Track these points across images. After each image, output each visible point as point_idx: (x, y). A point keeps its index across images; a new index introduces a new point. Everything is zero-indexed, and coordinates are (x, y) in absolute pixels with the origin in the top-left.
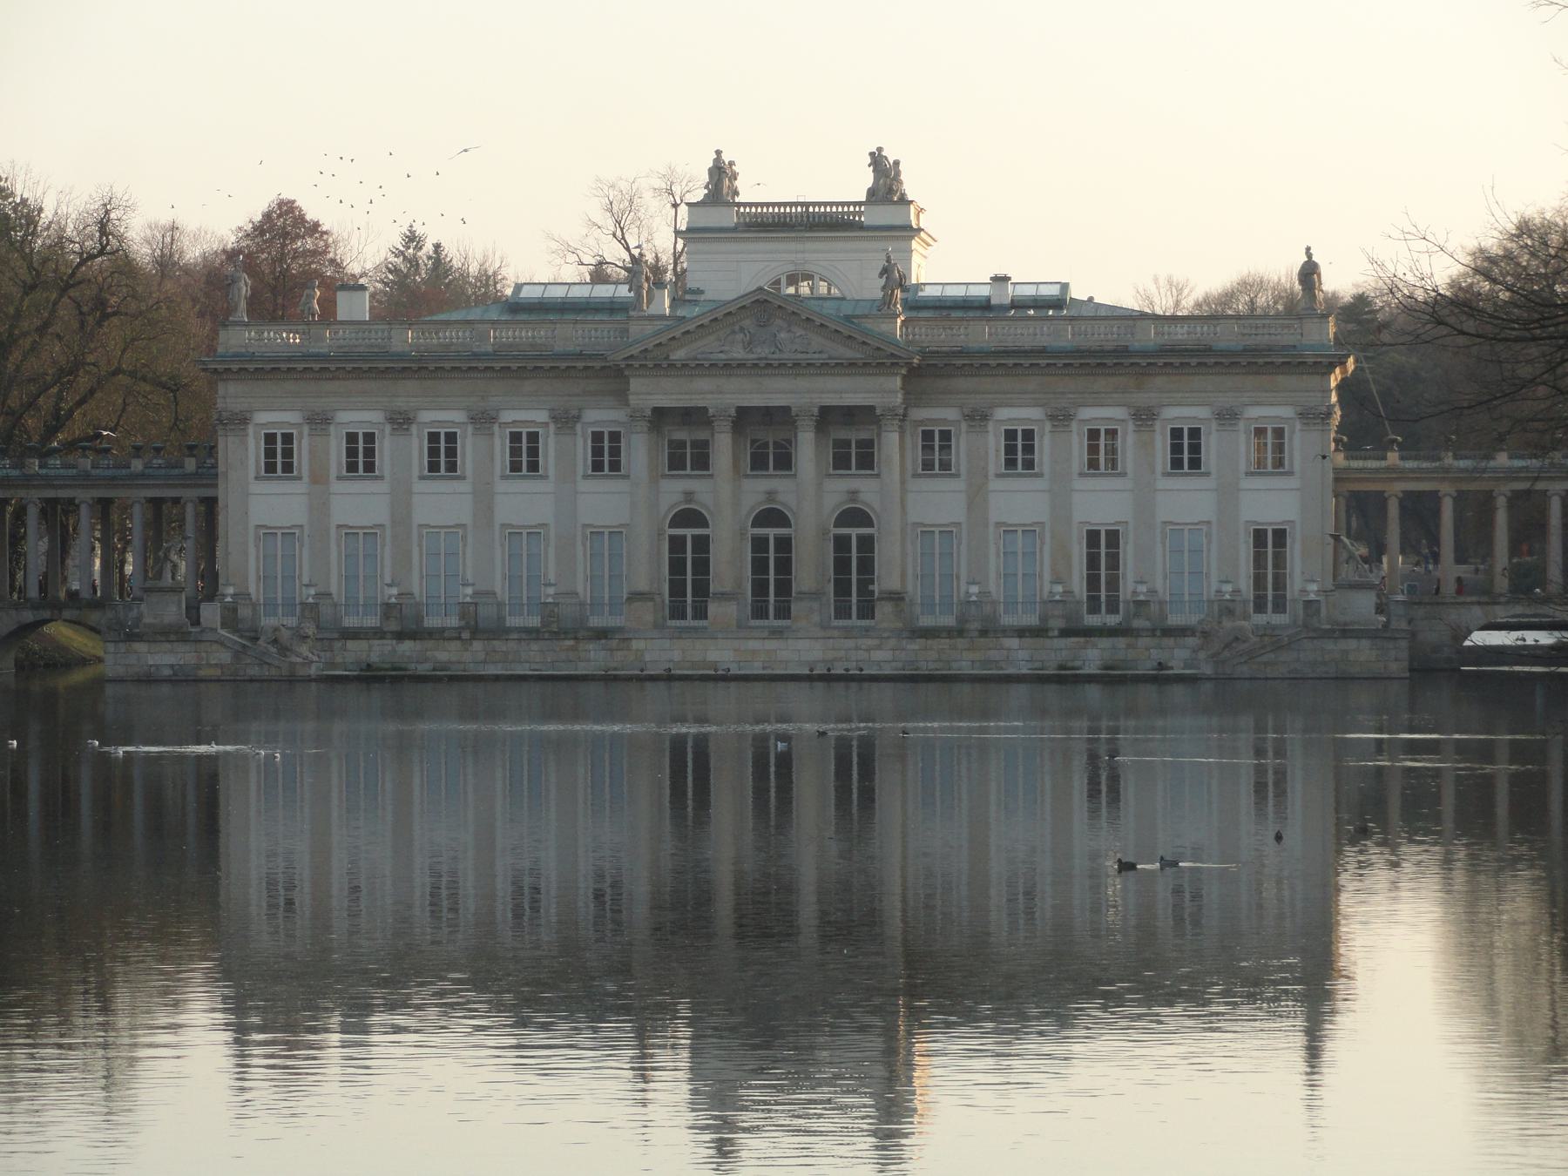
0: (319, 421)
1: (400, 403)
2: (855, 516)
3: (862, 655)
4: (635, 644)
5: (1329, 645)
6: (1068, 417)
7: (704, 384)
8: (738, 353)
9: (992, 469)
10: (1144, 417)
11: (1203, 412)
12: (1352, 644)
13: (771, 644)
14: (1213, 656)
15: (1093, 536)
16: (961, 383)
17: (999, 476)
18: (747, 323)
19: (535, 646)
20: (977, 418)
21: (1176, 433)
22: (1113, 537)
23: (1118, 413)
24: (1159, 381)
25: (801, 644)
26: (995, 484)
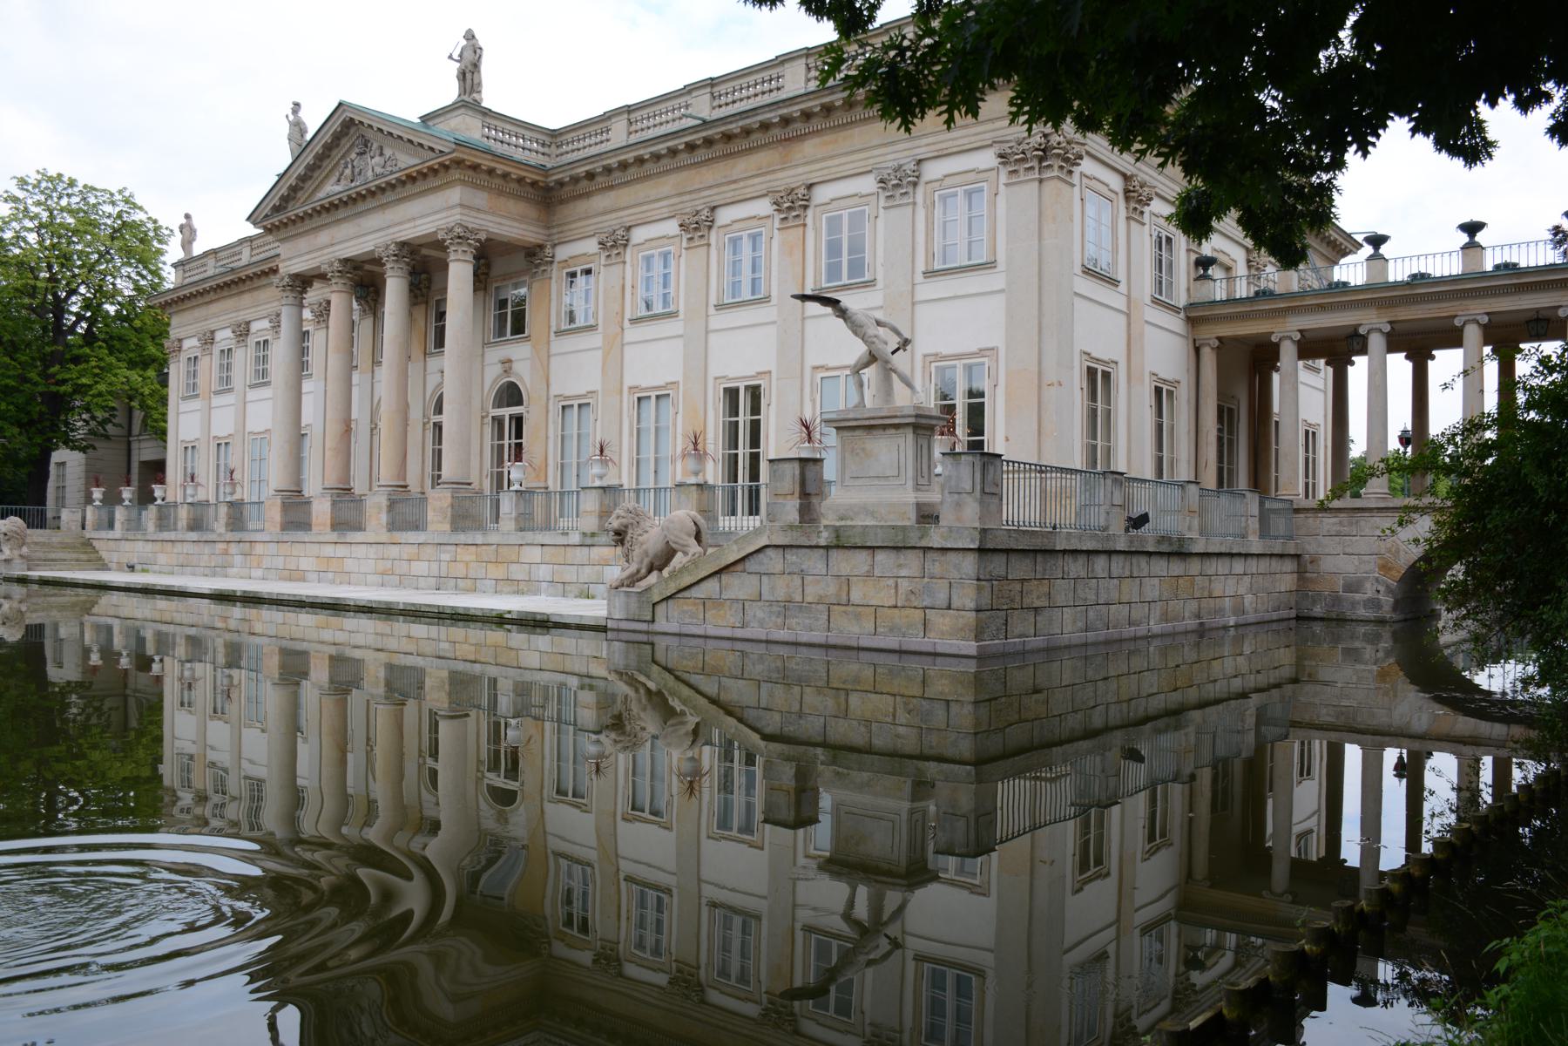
0: (208, 340)
1: (243, 316)
2: (511, 394)
3: (402, 567)
4: (259, 549)
5: (814, 562)
6: (711, 224)
7: (323, 237)
8: (332, 189)
9: (628, 315)
10: (793, 205)
12: (860, 560)
13: (341, 551)
14: (634, 579)
15: (732, 394)
16: (599, 202)
17: (634, 321)
18: (353, 156)
19: (207, 549)
20: (616, 244)
21: (834, 225)
22: (755, 393)
24: (810, 147)
25: (361, 551)
26: (632, 333)
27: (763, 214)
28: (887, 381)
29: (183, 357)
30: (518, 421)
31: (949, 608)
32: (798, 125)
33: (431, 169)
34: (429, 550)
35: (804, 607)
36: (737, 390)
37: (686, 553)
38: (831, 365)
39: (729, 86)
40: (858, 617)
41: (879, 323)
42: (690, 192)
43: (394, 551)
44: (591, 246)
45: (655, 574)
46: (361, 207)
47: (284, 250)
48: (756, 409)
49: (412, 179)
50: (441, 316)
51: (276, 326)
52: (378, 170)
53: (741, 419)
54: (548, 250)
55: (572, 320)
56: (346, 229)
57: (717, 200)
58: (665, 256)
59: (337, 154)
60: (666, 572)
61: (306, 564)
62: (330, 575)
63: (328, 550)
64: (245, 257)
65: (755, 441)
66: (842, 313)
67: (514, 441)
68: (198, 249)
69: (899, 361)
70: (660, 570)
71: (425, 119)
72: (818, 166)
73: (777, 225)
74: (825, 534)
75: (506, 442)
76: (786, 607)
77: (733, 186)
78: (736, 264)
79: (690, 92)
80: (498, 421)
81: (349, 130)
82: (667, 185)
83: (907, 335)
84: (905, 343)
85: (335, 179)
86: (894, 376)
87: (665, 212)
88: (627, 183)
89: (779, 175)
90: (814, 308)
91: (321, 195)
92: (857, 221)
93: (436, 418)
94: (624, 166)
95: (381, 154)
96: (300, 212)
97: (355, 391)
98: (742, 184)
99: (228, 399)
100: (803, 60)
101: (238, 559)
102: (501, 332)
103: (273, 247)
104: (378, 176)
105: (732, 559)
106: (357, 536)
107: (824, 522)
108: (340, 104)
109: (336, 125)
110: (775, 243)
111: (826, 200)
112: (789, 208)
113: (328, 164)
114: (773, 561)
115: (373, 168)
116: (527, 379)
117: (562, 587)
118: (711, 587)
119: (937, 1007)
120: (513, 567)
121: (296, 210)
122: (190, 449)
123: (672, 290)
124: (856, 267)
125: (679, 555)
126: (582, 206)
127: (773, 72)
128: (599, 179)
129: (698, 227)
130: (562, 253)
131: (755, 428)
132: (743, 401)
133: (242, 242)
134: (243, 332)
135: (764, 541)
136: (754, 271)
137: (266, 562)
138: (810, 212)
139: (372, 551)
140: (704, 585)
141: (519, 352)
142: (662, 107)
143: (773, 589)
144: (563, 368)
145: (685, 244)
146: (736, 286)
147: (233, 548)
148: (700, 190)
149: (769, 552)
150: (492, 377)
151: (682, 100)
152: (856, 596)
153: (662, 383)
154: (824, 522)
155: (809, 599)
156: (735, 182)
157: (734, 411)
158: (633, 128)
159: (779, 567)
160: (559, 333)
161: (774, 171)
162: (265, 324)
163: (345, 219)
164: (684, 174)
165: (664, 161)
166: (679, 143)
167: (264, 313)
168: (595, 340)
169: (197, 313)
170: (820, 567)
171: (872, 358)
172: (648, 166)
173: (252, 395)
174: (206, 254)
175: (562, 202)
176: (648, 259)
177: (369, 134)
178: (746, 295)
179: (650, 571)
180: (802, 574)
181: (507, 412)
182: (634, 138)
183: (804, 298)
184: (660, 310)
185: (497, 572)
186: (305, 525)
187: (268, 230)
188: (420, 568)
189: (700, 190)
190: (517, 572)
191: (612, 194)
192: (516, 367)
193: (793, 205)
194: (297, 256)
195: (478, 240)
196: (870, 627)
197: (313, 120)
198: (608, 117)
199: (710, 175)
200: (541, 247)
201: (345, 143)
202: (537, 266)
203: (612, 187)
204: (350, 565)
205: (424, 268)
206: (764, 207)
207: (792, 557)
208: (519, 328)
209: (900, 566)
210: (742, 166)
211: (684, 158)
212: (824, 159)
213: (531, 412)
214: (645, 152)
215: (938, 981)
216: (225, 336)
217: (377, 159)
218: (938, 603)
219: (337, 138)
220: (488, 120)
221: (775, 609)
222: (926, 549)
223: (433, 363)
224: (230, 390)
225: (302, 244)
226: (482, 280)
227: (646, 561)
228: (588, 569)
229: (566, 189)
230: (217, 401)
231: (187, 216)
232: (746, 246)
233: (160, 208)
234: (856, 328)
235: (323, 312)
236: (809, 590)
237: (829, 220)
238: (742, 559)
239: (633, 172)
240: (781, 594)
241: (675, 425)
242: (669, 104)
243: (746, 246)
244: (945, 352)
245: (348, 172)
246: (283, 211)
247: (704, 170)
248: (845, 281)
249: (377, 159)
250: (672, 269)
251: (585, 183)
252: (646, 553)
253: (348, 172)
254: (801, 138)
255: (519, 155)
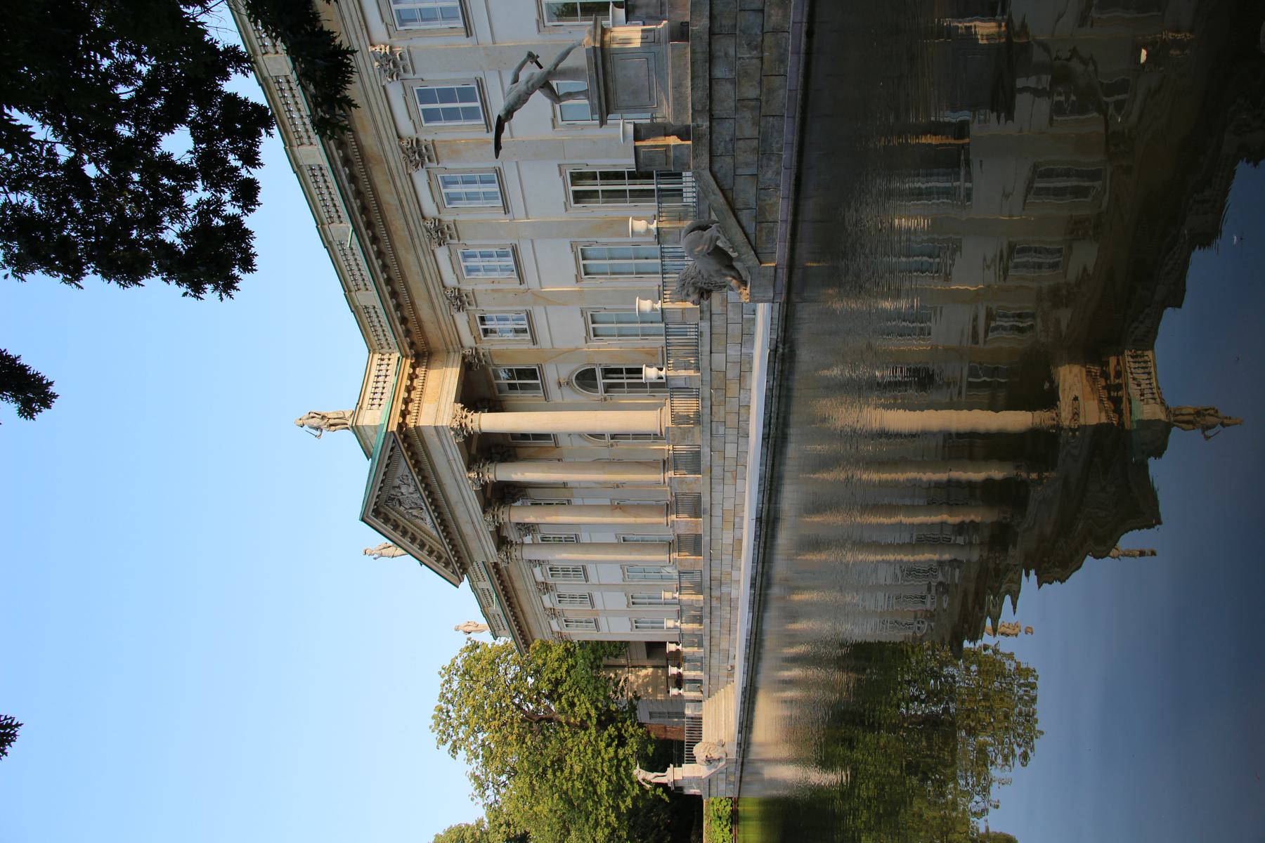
0: (553, 613)
1: (532, 587)
2: (586, 379)
3: (730, 464)
4: (716, 574)
5: (725, 131)
7: (467, 529)
8: (427, 523)
11: (395, 91)
13: (717, 511)
15: (579, 197)
16: (425, 312)
17: (521, 281)
19: (716, 613)
20: (459, 300)
21: (430, 116)
22: (577, 177)
23: (420, 178)
24: (368, 140)
25: (717, 497)
27: (426, 177)
28: (566, 74)
29: (565, 631)
30: (608, 372)
31: (762, 11)
32: (350, 152)
33: (407, 450)
34: (715, 443)
35: (763, 138)
36: (575, 192)
37: (718, 238)
38: (551, 115)
39: (322, 210)
40: (771, 91)
41: (516, 80)
42: (412, 239)
43: (717, 471)
44: (461, 319)
45: (736, 264)
46: (442, 502)
47: (479, 558)
48: (593, 176)
49: (417, 464)
50: (525, 436)
51: (539, 563)
52: (412, 489)
53: (600, 188)
54: (467, 352)
55: (525, 331)
56: (460, 512)
57: (417, 215)
58: (466, 256)
59: (402, 522)
60: (734, 255)
61: (727, 537)
62: (737, 520)
63: (717, 521)
64: (486, 585)
65: (618, 176)
66: (509, 113)
67: (624, 375)
68: (482, 621)
69: (547, 63)
70: (731, 259)
71: (368, 455)
72: (382, 132)
73: (434, 165)
74: (699, 121)
75: (625, 381)
76: (764, 153)
77: (405, 203)
78: (471, 197)
79: (330, 243)
80: (608, 387)
81: (381, 510)
82: (408, 258)
83: (525, 56)
84: (532, 57)
85: (419, 521)
86: (561, 66)
87: (430, 258)
88: (408, 291)
89: (393, 164)
90: (505, 136)
91: (435, 533)
92: (425, 96)
93: (608, 438)
94: (394, 294)
95: (399, 487)
96: (448, 548)
97: (588, 502)
98: (402, 196)
99: (597, 597)
100: (295, 149)
101: (725, 589)
102: (536, 387)
103: (477, 567)
104: (417, 489)
105: (721, 200)
106: (705, 499)
107: (689, 122)
108: (363, 520)
109: (379, 523)
110: (450, 166)
111: (411, 124)
112: (420, 155)
113: (411, 529)
114: (724, 164)
115: (409, 491)
116: (574, 367)
117: (747, 336)
118: (745, 216)
119: (1059, 192)
120: (729, 375)
121: (446, 550)
122: (637, 625)
123: (494, 250)
124: (466, 95)
125: (719, 244)
126: (430, 327)
127: (308, 174)
128: (406, 314)
129: (441, 233)
130: (468, 340)
131: (606, 176)
132: (586, 186)
133: (474, 589)
134: (546, 588)
135: (707, 174)
136: (475, 182)
137: (727, 568)
138: (422, 138)
139: (717, 488)
140: (745, 222)
141: (552, 374)
142: (344, 264)
143: (747, 165)
144: (563, 337)
145: (456, 241)
146: (488, 196)
147: (716, 593)
148: (410, 231)
149: (716, 167)
150: (571, 396)
151: (337, 249)
152: (752, 93)
153: (572, 256)
154: (689, 122)
155: (756, 134)
156: (401, 202)
157: (591, 195)
158: (362, 286)
159: (728, 160)
160: (534, 340)
161: (390, 169)
162: (537, 571)
163: (452, 513)
164: (397, 244)
165: (388, 262)
166: (372, 250)
167: (529, 572)
168: (539, 314)
169: (531, 621)
170: (728, 124)
171: (545, 85)
172: (393, 275)
173: (593, 579)
174: (486, 615)
175: (427, 343)
176: (470, 270)
177: (384, 497)
178: (494, 188)
179: (733, 268)
180: (734, 140)
181: (601, 381)
182: (371, 286)
183: (498, 147)
184: (511, 258)
185: (733, 388)
186: (697, 539)
187: (465, 571)
188: (731, 450)
189: (410, 231)
190: (732, 373)
191: (417, 302)
192: (564, 377)
193: (418, 154)
194: (483, 549)
195: (463, 409)
196: (777, 81)
197: (377, 540)
198: (355, 309)
199: (397, 224)
200: (464, 357)
201: (393, 515)
202: (480, 360)
203: (412, 303)
204: (728, 505)
205: (486, 449)
206: (420, 178)
207: (720, 149)
208: (532, 374)
209: (726, 55)
210: (388, 198)
211: (385, 245)
212: (377, 128)
213: (599, 363)
214: (382, 278)
215: (1040, 192)
216: (547, 601)
217: (404, 490)
218: (759, 20)
219: (387, 520)
220: (365, 406)
221: (765, 161)
222: (711, 33)
223: (564, 442)
224: (590, 596)
225: (473, 545)
226: (496, 405)
227: (724, 271)
228: (731, 315)
229: (416, 340)
230: (599, 605)
231: (457, 629)
232: (453, 189)
233: (452, 648)
234: (521, 100)
235: (528, 528)
236: (748, 133)
237: (427, 120)
238: (722, 191)
239: (400, 288)
240: (751, 158)
241: (606, 244)
242: (341, 259)
243: (453, 189)
244: (536, 16)
245: (415, 512)
246: (451, 559)
247: (393, 228)
248: (478, 104)
249: (404, 490)
250: (477, 250)
251: (409, 325)
252: (718, 271)
253: (415, 512)
254: (360, 148)
255: (392, 379)
